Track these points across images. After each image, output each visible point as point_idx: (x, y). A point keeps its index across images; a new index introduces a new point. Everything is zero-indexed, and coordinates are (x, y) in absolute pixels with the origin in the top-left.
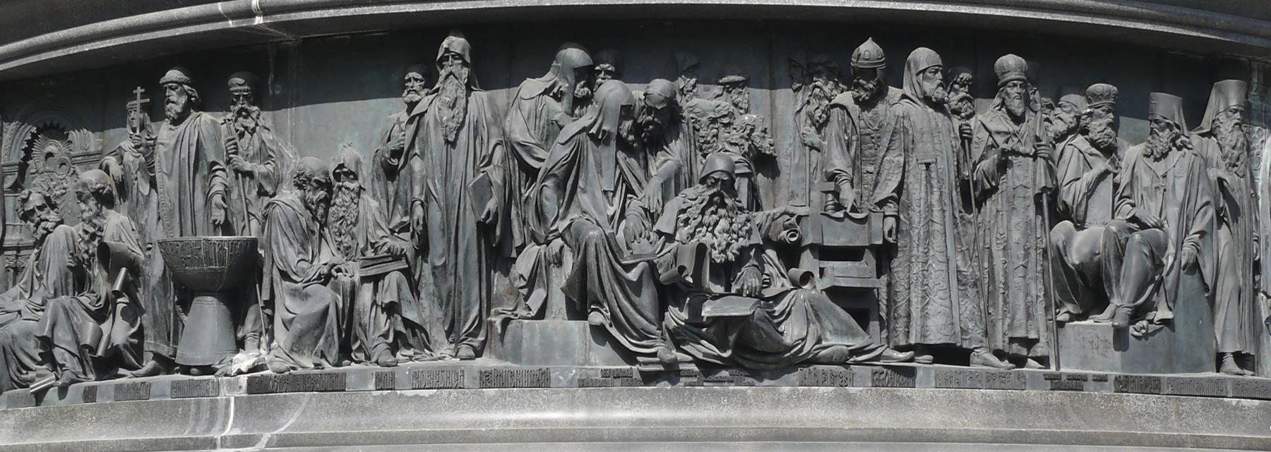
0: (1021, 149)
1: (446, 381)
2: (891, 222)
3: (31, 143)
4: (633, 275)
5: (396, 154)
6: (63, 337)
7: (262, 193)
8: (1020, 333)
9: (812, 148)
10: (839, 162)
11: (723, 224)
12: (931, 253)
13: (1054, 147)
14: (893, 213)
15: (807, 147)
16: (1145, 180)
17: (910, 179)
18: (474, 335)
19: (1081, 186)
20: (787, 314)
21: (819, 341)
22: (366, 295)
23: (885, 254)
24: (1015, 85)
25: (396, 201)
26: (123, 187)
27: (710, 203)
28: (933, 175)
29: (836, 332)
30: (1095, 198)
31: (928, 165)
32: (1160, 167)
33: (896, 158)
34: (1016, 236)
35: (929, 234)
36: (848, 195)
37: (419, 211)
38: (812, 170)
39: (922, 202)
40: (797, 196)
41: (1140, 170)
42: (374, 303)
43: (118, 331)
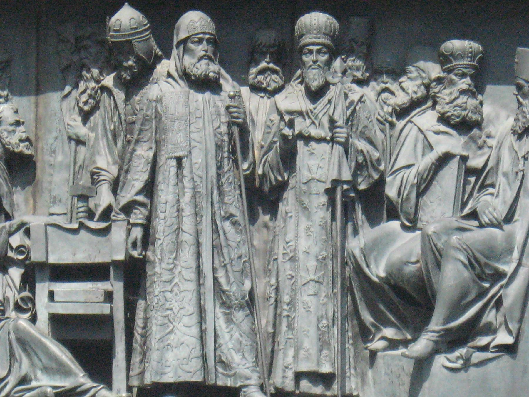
0: (314, 132)
2: (137, 233)
9: (79, 142)
12: (179, 269)
13: (392, 125)
14: (140, 221)
15: (73, 143)
16: (506, 164)
17: (160, 178)
19: (411, 176)
24: (311, 52)
28: (186, 171)
29: (46, 370)
30: (436, 189)
31: (179, 160)
35: (178, 246)
38: (77, 169)
39: (168, 206)
40: (60, 201)
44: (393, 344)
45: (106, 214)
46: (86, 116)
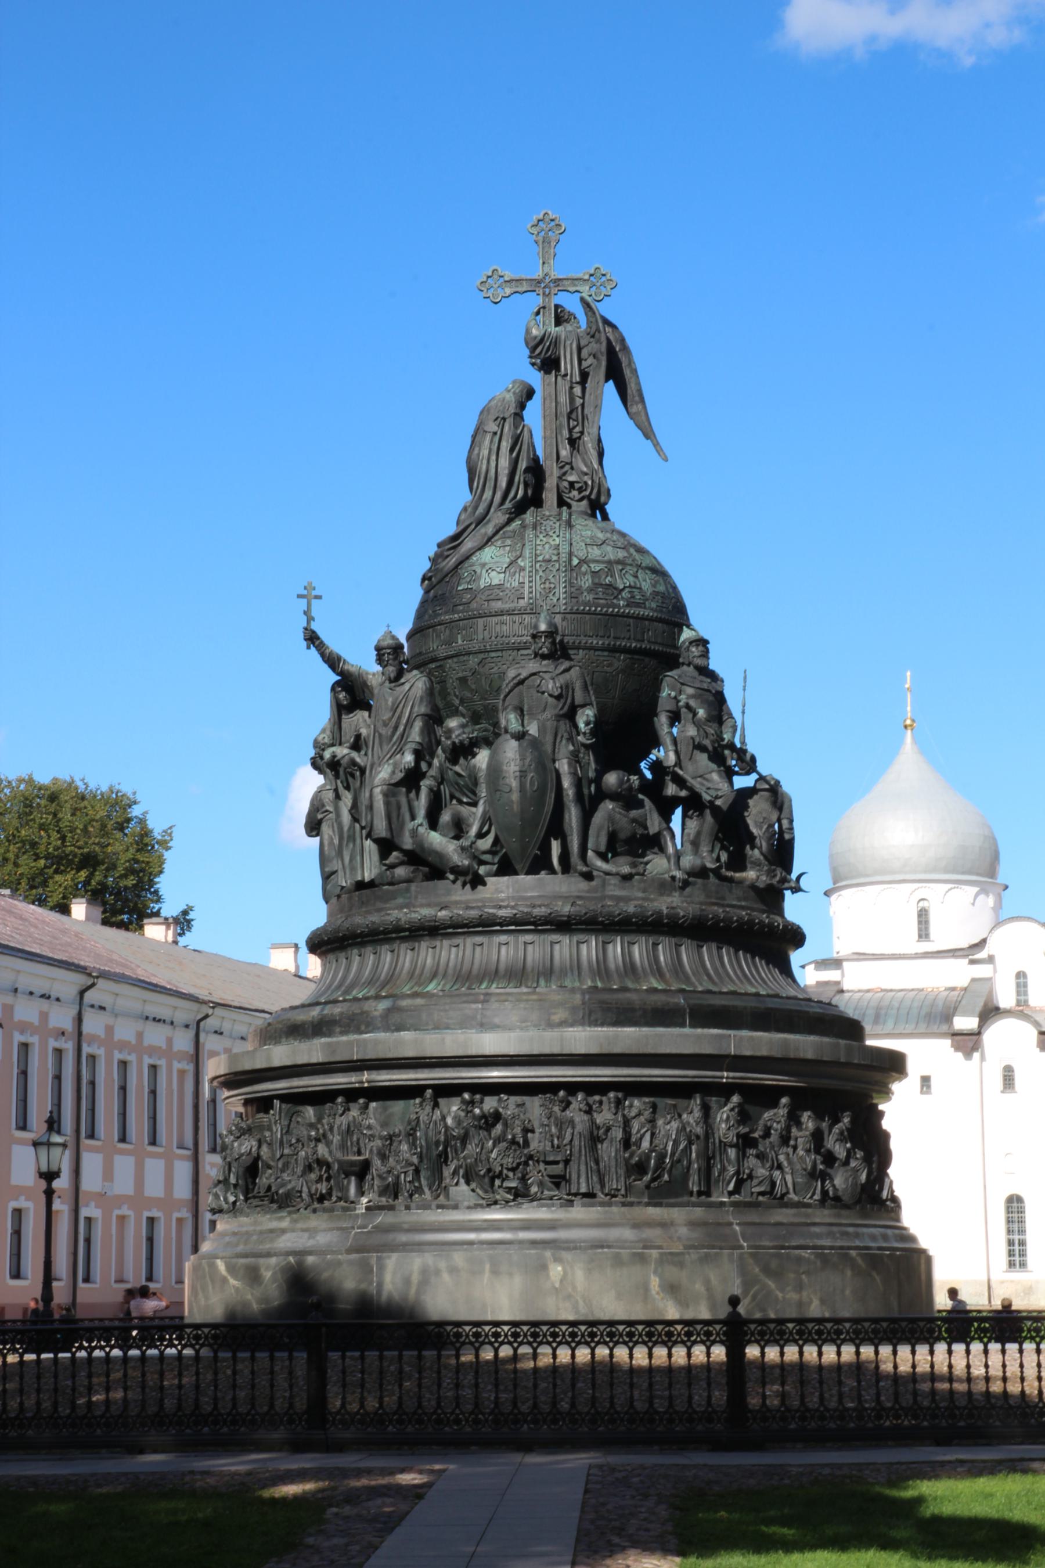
1: (426, 1207)
2: (568, 1152)
3: (291, 1117)
4: (482, 1173)
5: (411, 1129)
6: (305, 1189)
7: (369, 1140)
8: (615, 1187)
9: (546, 1125)
10: (554, 1130)
11: (512, 1155)
17: (575, 1137)
18: (437, 1190)
20: (532, 1184)
21: (542, 1193)
22: (403, 1176)
23: (567, 1162)
25: (413, 1145)
26: (324, 1135)
27: (507, 1148)
32: (668, 1127)
33: (569, 1131)
34: (613, 1154)
35: (580, 1155)
36: (556, 1142)
37: (419, 1150)
41: (662, 1129)
42: (405, 1181)
43: (323, 1188)
44: (635, 1180)
45: (558, 1147)
46: (549, 1118)
